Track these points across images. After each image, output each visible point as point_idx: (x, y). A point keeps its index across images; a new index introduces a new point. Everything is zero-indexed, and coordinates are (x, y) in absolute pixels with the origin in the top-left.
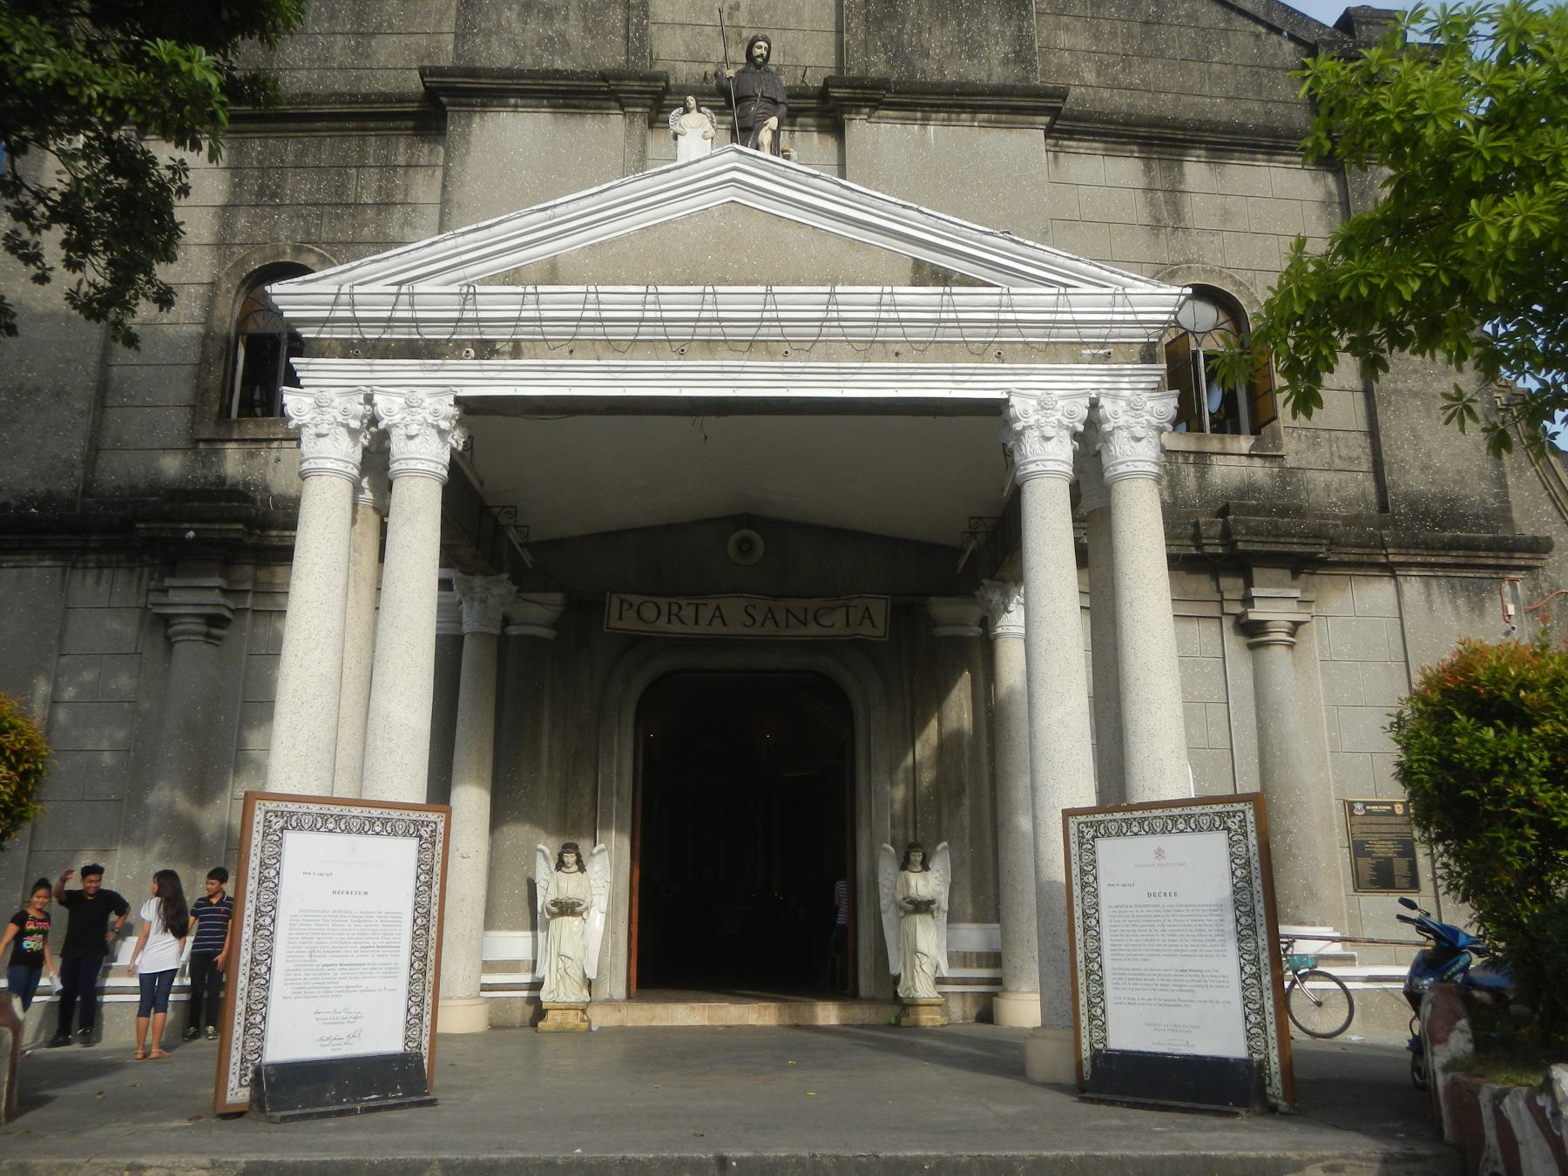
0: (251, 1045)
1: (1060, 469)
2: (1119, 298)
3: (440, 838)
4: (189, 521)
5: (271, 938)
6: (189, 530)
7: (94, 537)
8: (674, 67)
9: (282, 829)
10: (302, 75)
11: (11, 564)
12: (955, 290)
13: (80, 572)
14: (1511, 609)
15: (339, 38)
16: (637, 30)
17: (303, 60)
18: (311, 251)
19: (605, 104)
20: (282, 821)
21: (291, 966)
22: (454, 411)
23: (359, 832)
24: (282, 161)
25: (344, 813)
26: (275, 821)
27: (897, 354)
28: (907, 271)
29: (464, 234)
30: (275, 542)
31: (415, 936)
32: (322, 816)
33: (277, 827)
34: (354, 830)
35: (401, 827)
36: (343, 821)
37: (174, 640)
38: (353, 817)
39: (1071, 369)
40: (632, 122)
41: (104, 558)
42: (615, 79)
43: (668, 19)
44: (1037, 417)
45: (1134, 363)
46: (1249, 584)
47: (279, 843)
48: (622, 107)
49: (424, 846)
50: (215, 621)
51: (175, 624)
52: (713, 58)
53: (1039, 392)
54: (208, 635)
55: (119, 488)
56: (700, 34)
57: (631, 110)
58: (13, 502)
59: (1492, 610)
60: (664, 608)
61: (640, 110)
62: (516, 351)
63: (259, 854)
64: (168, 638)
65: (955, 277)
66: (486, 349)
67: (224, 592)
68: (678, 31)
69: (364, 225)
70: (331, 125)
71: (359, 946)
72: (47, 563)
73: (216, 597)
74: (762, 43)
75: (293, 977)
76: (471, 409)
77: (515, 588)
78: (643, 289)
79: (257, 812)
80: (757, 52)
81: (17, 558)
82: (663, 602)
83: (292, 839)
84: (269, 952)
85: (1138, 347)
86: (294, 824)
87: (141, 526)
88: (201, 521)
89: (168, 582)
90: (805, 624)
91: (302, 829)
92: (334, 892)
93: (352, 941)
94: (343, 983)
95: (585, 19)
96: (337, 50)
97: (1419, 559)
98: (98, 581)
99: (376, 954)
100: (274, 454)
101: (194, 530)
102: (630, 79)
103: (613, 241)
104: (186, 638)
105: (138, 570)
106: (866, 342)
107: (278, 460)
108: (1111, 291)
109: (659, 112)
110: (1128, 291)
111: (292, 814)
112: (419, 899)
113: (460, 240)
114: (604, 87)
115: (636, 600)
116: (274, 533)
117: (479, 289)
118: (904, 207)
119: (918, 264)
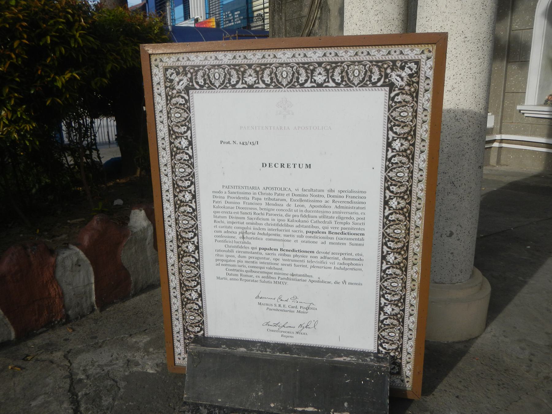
5: (194, 215)
9: (187, 89)
20: (185, 79)
21: (222, 246)
23: (291, 85)
25: (269, 60)
26: (177, 79)
31: (387, 223)
33: (181, 87)
34: (285, 83)
36: (267, 72)
38: (281, 64)
47: (187, 108)
49: (399, 98)
63: (165, 121)
71: (305, 230)
75: (225, 258)
79: (155, 70)
86: (201, 81)
91: (211, 86)
92: (264, 165)
93: (295, 224)
94: (287, 270)
99: (328, 241)
111: (196, 69)
112: (391, 174)
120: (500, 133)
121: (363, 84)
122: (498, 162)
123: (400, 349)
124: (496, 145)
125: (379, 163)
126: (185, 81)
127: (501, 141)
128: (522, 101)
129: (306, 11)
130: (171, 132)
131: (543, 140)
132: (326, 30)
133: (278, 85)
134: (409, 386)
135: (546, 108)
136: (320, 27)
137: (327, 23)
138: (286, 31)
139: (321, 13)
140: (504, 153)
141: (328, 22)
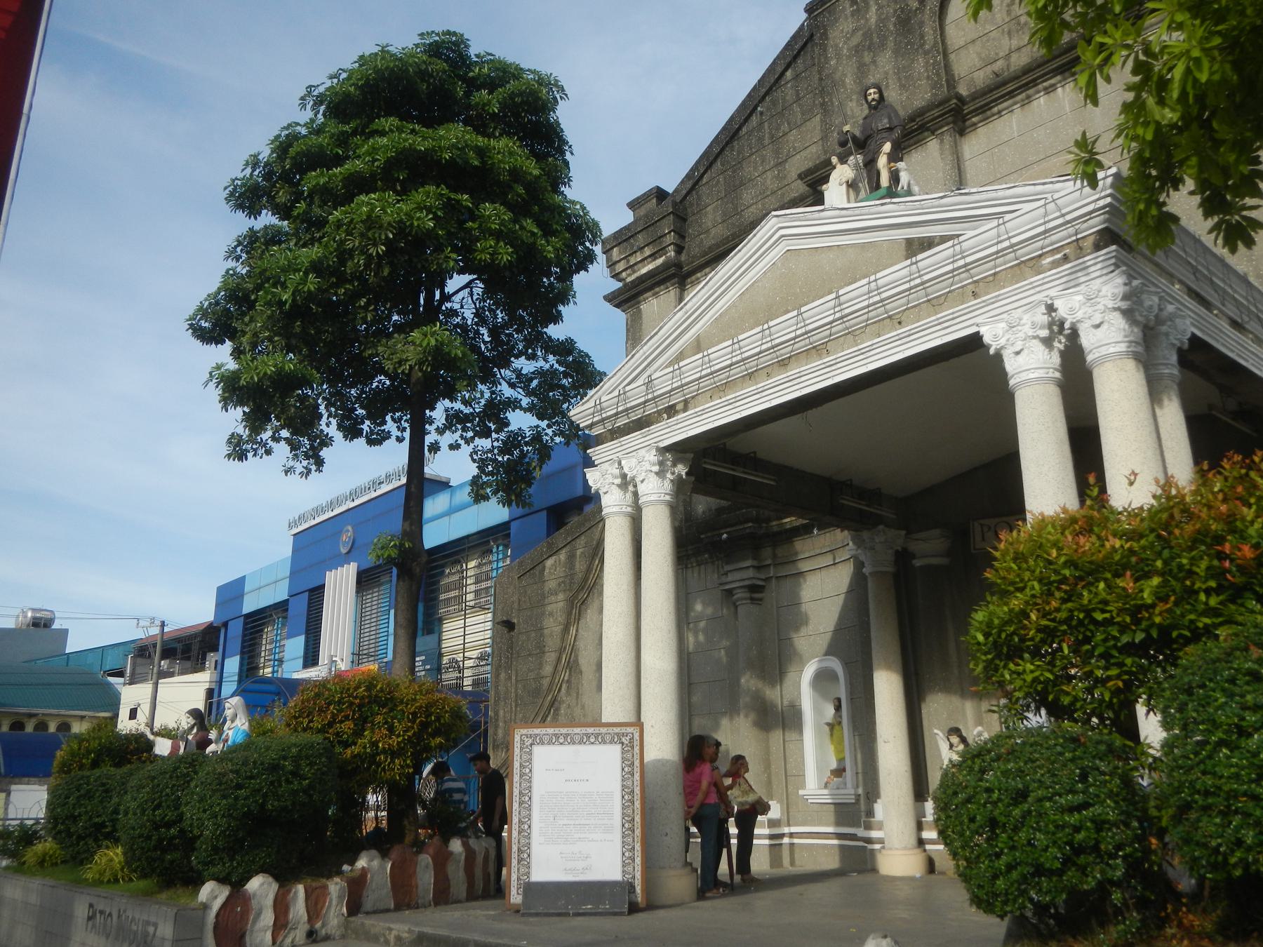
0: (522, 870)
1: (1036, 375)
2: (1051, 206)
3: (637, 743)
5: (529, 809)
8: (973, 79)
9: (531, 745)
12: (920, 257)
13: (690, 571)
15: (768, 173)
16: (934, 68)
19: (920, 137)
23: (580, 743)
27: (900, 323)
29: (646, 343)
30: (775, 529)
32: (555, 735)
35: (608, 738)
39: (1031, 283)
40: (942, 141)
42: (919, 116)
43: (962, 43)
44: (1007, 336)
45: (1089, 254)
47: (530, 753)
48: (933, 133)
50: (754, 589)
52: (1001, 54)
53: (1005, 316)
54: (752, 599)
56: (988, 41)
57: (939, 132)
61: (946, 128)
62: (686, 405)
65: (936, 241)
66: (671, 411)
67: (758, 568)
68: (971, 48)
73: (751, 573)
74: (872, 91)
76: (678, 450)
77: (903, 533)
78: (730, 342)
80: (870, 98)
83: (537, 750)
84: (529, 817)
85: (1092, 239)
87: (702, 536)
88: (726, 527)
91: (543, 744)
94: (576, 836)
95: (899, 79)
96: (769, 182)
98: (699, 573)
102: (929, 111)
103: (726, 310)
106: (862, 328)
108: (1042, 202)
109: (964, 121)
110: (1055, 197)
111: (536, 735)
113: (645, 348)
114: (914, 125)
116: (774, 523)
118: (882, 204)
119: (909, 242)
120: (789, 825)
121: (611, 743)
122: (792, 863)
123: (634, 877)
124: (786, 840)
125: (619, 778)
126: (530, 741)
127: (791, 835)
128: (803, 786)
129: (548, 669)
130: (521, 765)
131: (830, 829)
132: (577, 698)
133: (574, 743)
134: (639, 899)
135: (826, 792)
136: (568, 693)
138: (516, 696)
139: (570, 674)
140: (797, 851)
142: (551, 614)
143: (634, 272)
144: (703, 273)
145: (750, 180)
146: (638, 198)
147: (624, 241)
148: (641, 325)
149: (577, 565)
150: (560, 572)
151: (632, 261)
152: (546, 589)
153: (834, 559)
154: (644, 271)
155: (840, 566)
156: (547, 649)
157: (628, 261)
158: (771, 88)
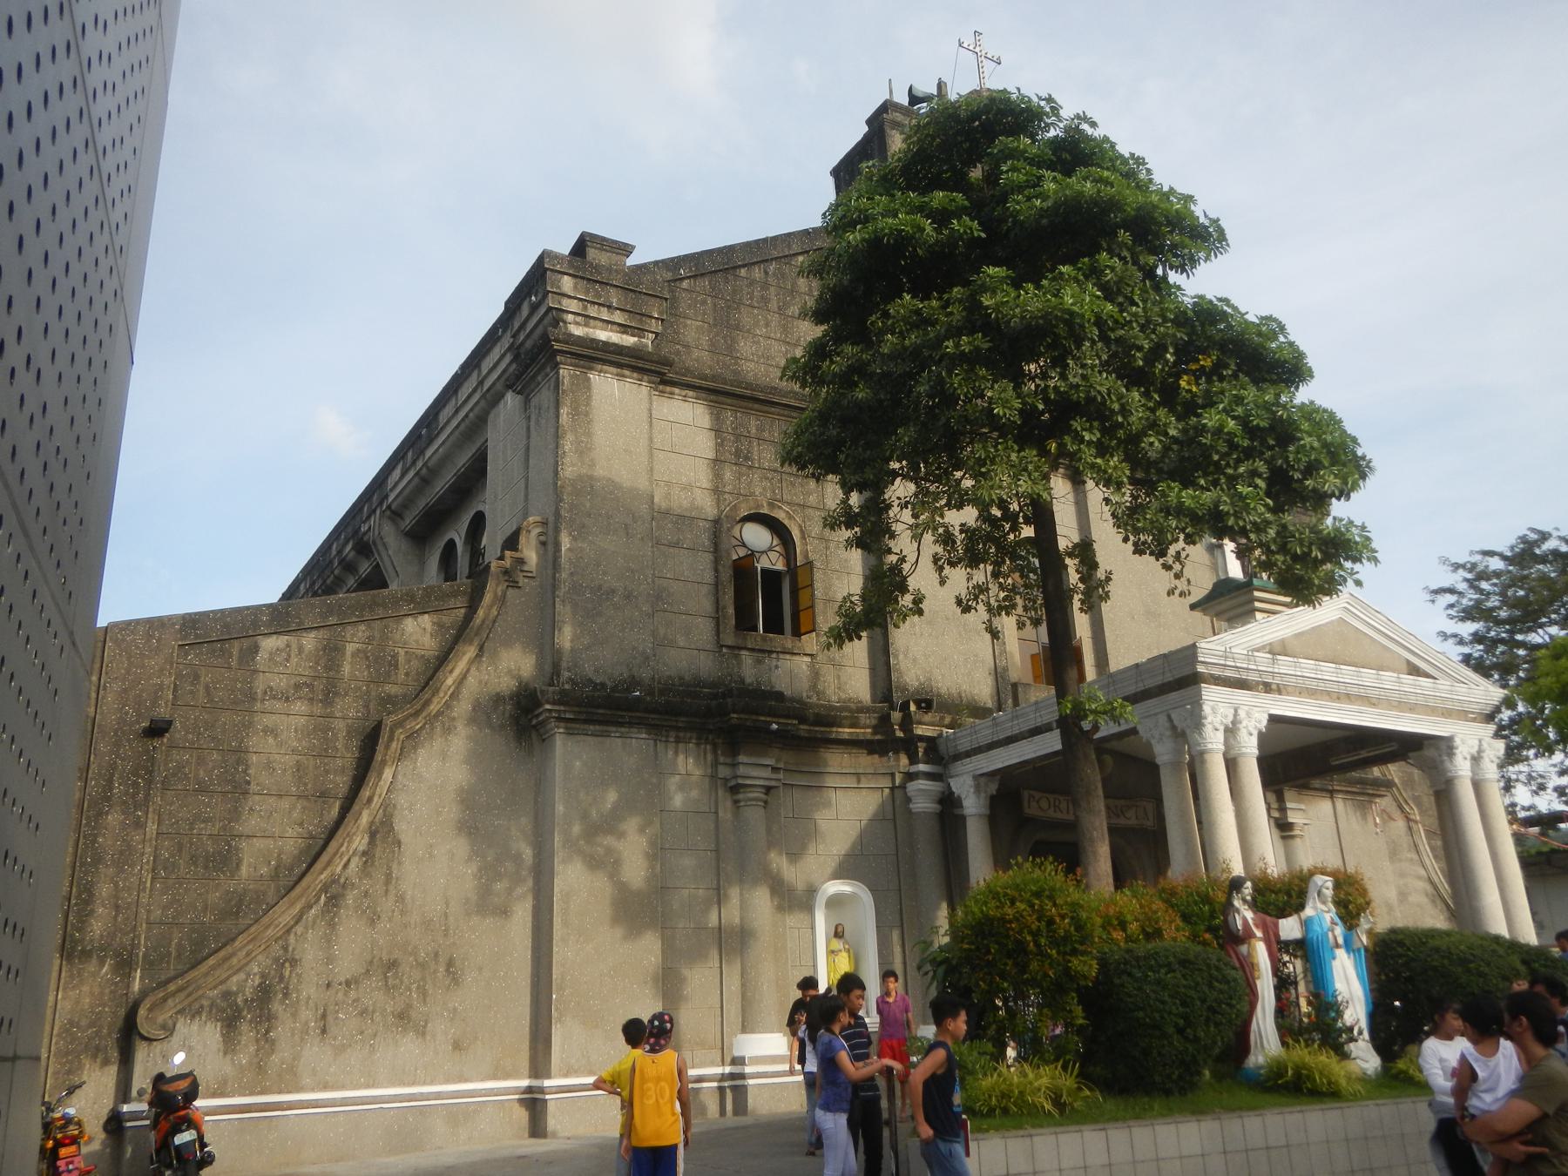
4: (769, 716)
6: (771, 723)
7: (683, 719)
10: (752, 365)
11: (617, 735)
14: (1378, 820)
17: (753, 354)
18: (780, 508)
22: (1265, 722)
24: (749, 432)
28: (1404, 667)
37: (742, 804)
41: (681, 734)
46: (1281, 799)
51: (744, 792)
54: (766, 802)
55: (670, 677)
58: (609, 684)
59: (1370, 819)
60: (1052, 800)
64: (736, 802)
66: (1267, 688)
69: (809, 493)
70: (782, 412)
72: (644, 736)
73: (767, 773)
81: (623, 729)
82: (1052, 797)
87: (735, 716)
88: (775, 716)
89: (742, 758)
90: (1118, 816)
97: (1344, 789)
100: (774, 663)
101: (777, 723)
104: (754, 803)
105: (703, 746)
107: (777, 667)
115: (1037, 795)
117: (1256, 654)
119: (1408, 662)
137: (389, 868)
141: (395, 866)
142: (271, 731)
143: (586, 325)
144: (684, 393)
145: (748, 331)
146: (604, 239)
147: (589, 280)
148: (589, 398)
149: (346, 669)
150: (301, 667)
151: (593, 311)
152: (260, 684)
153: (859, 782)
154: (603, 335)
155: (864, 792)
156: (253, 788)
157: (585, 308)
158: (781, 257)
